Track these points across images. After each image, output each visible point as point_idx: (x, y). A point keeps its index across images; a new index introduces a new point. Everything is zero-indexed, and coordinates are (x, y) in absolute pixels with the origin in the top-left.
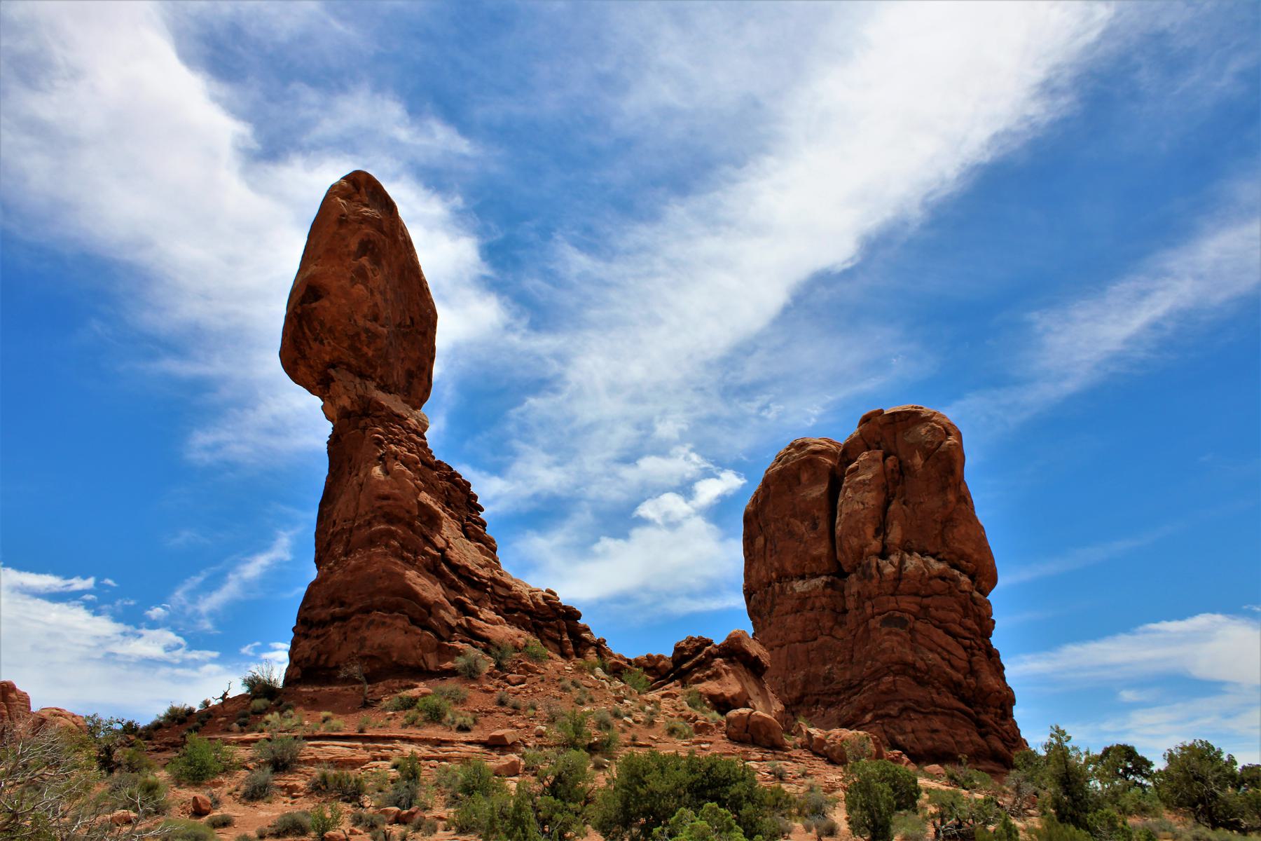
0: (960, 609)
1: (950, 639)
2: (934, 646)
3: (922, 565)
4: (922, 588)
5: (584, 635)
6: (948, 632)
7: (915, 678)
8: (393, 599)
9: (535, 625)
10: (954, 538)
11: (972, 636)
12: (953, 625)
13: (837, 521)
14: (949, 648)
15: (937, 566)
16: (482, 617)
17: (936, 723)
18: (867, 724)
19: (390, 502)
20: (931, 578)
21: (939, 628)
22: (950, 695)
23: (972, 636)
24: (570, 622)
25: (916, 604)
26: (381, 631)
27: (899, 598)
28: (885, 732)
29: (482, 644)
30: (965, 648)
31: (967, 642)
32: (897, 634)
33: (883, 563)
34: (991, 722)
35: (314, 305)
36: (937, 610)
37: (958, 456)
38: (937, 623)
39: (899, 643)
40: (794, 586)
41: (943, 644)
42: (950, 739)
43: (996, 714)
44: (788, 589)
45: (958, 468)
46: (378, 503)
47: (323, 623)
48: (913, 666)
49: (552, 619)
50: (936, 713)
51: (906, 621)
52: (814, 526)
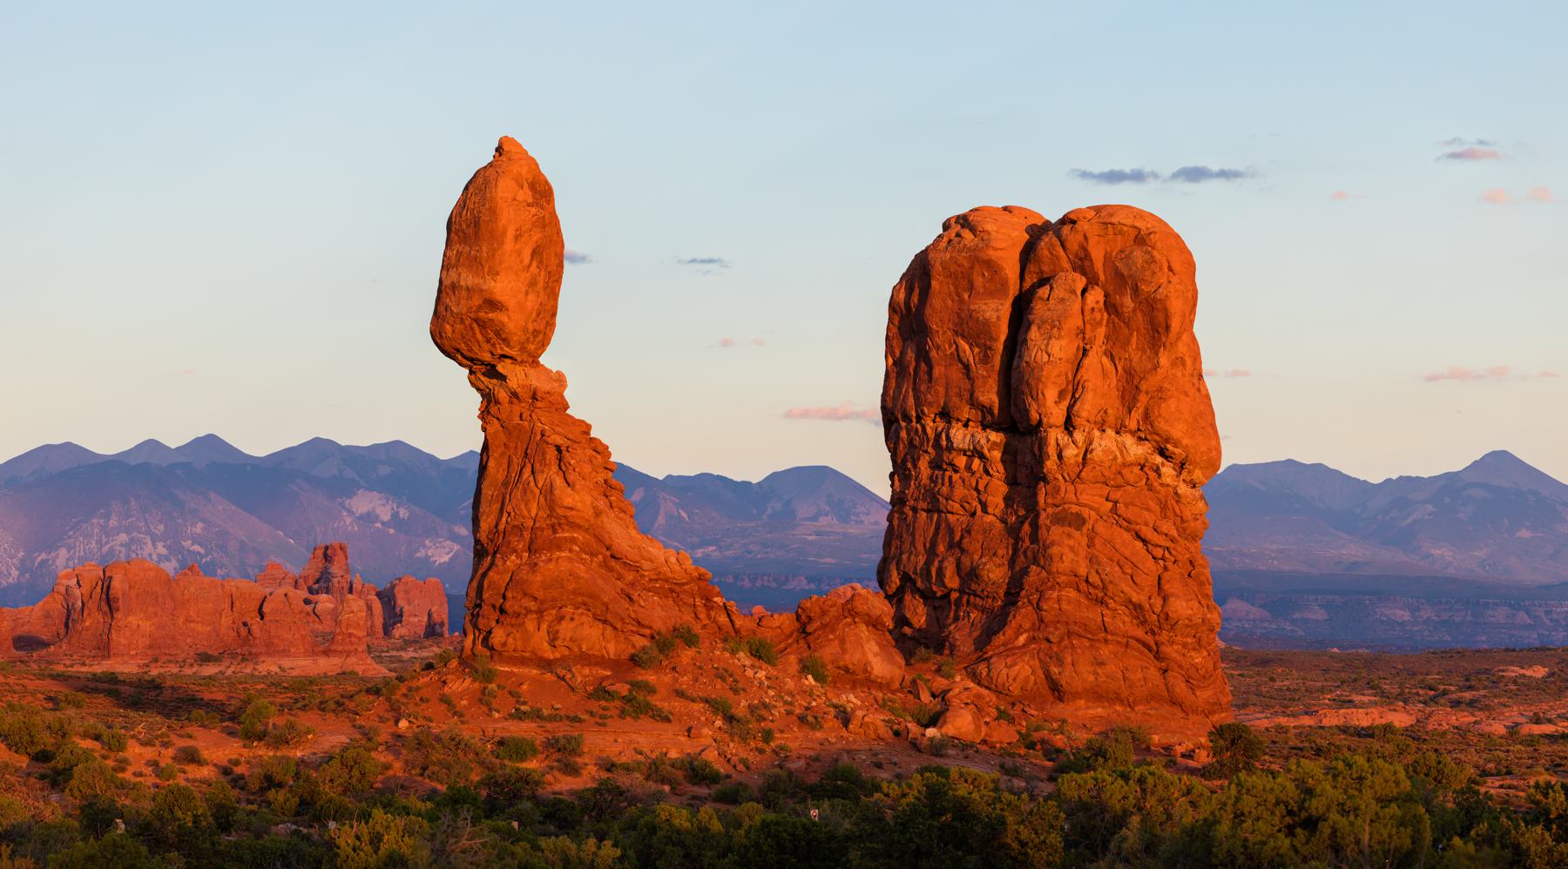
0: (1157, 509)
1: (1139, 544)
2: (1117, 557)
3: (1115, 448)
4: (1115, 478)
5: (715, 599)
6: (1138, 536)
7: (1088, 595)
8: (580, 599)
9: (672, 591)
10: (1160, 415)
11: (1168, 544)
12: (1144, 528)
13: (1015, 363)
14: (1134, 560)
15: (1136, 450)
16: (642, 604)
17: (1105, 651)
18: (1020, 648)
19: (574, 513)
20: (1125, 465)
21: (1127, 530)
22: (1127, 619)
23: (1168, 544)
24: (702, 584)
25: (1101, 496)
26: (572, 625)
27: (1081, 487)
28: (1040, 660)
29: (647, 632)
30: (1154, 558)
31: (1159, 552)
32: (1070, 536)
33: (1064, 438)
34: (1175, 655)
35: (491, 315)
36: (1126, 506)
37: (1176, 306)
38: (1125, 524)
39: (1071, 548)
40: (951, 435)
41: (1127, 553)
42: (1120, 675)
43: (1185, 646)
44: (944, 436)
45: (1175, 324)
46: (561, 512)
47: (518, 615)
48: (1087, 581)
49: (687, 584)
50: (1106, 641)
51: (1084, 519)
52: (986, 359)
